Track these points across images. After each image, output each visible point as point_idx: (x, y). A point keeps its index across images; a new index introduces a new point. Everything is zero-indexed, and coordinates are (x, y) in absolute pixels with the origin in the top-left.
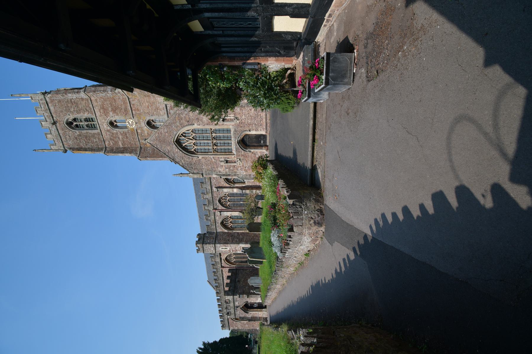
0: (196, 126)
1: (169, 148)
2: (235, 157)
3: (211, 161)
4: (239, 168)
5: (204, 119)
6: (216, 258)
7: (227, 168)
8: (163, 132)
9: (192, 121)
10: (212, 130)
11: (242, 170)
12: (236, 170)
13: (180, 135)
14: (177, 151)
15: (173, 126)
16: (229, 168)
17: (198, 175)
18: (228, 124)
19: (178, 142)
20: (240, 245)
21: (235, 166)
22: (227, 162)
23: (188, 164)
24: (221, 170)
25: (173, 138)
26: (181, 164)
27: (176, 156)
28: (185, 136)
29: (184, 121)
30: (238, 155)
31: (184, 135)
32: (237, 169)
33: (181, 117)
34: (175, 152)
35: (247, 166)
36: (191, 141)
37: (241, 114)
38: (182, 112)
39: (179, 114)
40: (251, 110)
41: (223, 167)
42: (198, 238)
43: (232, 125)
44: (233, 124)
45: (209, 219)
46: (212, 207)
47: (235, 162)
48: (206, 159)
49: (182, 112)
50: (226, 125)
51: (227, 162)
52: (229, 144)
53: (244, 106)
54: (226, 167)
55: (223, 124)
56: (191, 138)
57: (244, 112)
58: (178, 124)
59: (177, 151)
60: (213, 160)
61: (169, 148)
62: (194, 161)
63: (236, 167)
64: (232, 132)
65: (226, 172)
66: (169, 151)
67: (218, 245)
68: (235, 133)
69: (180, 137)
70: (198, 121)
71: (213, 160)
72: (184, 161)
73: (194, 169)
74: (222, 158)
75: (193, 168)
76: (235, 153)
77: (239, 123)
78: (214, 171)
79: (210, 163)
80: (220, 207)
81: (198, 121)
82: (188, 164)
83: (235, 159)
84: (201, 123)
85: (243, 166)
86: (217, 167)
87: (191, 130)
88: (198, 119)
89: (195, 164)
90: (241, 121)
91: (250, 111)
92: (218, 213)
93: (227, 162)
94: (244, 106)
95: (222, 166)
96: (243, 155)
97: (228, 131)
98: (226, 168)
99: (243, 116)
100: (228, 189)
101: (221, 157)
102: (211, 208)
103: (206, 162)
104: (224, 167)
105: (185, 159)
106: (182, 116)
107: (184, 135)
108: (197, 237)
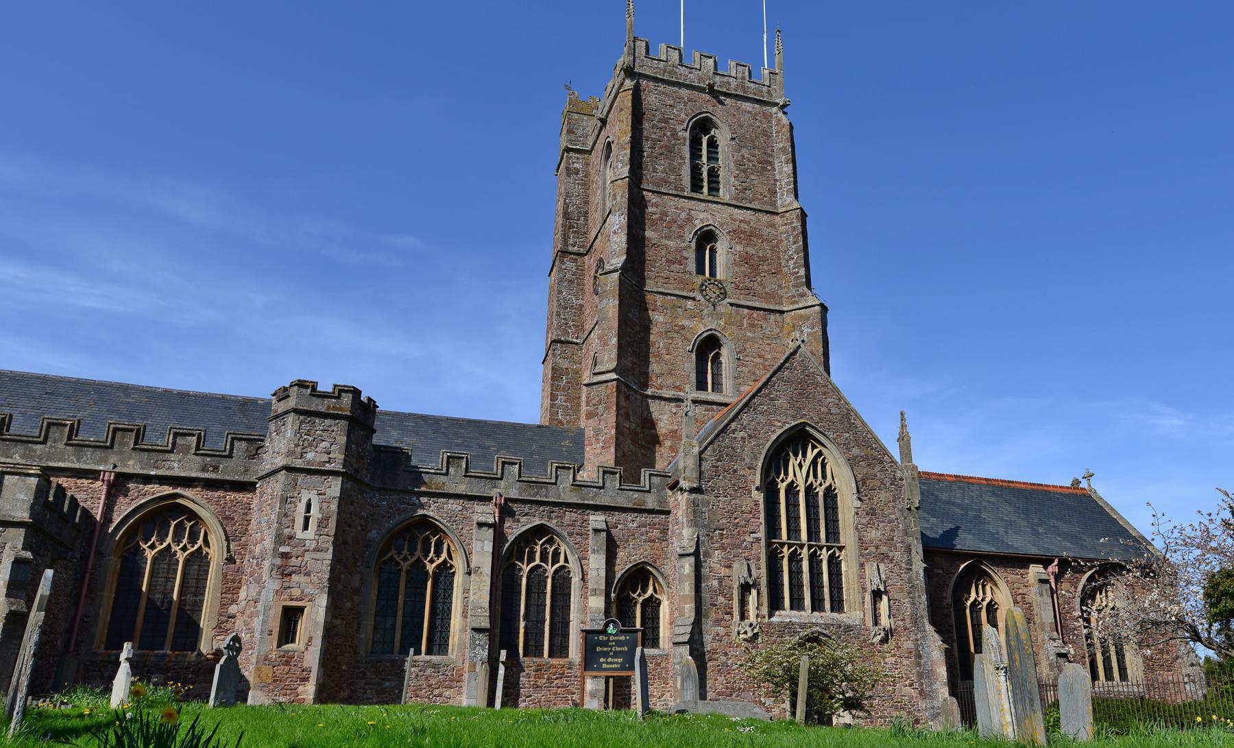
0: (848, 503)
1: (782, 402)
3: (745, 529)
4: (721, 630)
5: (874, 532)
6: (199, 459)
7: (720, 583)
8: (829, 400)
9: (866, 496)
10: (837, 551)
11: (714, 639)
13: (820, 448)
14: (774, 426)
15: (848, 435)
17: (695, 475)
18: (866, 607)
20: (325, 596)
21: (731, 614)
22: (745, 588)
23: (733, 448)
24: (715, 560)
25: (813, 424)
26: (733, 425)
27: (760, 417)
28: (814, 462)
29: (865, 471)
31: (820, 460)
32: (718, 622)
33: (875, 465)
34: (772, 417)
35: (730, 662)
37: (897, 653)
38: (887, 470)
39: (881, 462)
40: (911, 685)
41: (727, 570)
42: (331, 390)
43: (864, 620)
44: (867, 622)
45: (452, 470)
46: (514, 494)
47: (743, 617)
48: (751, 512)
49: (887, 470)
50: (863, 598)
52: (797, 604)
53: (919, 664)
55: (864, 589)
56: (811, 478)
57: (905, 662)
58: (855, 451)
59: (774, 426)
60: (749, 539)
61: (782, 402)
62: (742, 472)
63: (727, 617)
64: (835, 615)
66: (772, 400)
67: (334, 487)
68: (840, 627)
70: (867, 514)
71: (749, 539)
72: (743, 438)
73: (718, 467)
75: (718, 460)
76: (774, 619)
77: (873, 644)
78: (708, 535)
79: (736, 525)
80: (513, 530)
81: (867, 514)
82: (733, 448)
84: (864, 521)
85: (730, 645)
86: (723, 548)
87: (833, 483)
88: (874, 514)
89: (735, 471)
90: (879, 652)
91: (907, 683)
92: (487, 513)
93: (745, 588)
94: (919, 664)
95: (729, 567)
97: (837, 605)
98: (720, 580)
99: (894, 659)
100: (603, 573)
101: (759, 569)
102: (509, 488)
103: (743, 512)
104: (724, 572)
105: (750, 442)
106: (878, 468)
107: (820, 460)
108: (335, 386)
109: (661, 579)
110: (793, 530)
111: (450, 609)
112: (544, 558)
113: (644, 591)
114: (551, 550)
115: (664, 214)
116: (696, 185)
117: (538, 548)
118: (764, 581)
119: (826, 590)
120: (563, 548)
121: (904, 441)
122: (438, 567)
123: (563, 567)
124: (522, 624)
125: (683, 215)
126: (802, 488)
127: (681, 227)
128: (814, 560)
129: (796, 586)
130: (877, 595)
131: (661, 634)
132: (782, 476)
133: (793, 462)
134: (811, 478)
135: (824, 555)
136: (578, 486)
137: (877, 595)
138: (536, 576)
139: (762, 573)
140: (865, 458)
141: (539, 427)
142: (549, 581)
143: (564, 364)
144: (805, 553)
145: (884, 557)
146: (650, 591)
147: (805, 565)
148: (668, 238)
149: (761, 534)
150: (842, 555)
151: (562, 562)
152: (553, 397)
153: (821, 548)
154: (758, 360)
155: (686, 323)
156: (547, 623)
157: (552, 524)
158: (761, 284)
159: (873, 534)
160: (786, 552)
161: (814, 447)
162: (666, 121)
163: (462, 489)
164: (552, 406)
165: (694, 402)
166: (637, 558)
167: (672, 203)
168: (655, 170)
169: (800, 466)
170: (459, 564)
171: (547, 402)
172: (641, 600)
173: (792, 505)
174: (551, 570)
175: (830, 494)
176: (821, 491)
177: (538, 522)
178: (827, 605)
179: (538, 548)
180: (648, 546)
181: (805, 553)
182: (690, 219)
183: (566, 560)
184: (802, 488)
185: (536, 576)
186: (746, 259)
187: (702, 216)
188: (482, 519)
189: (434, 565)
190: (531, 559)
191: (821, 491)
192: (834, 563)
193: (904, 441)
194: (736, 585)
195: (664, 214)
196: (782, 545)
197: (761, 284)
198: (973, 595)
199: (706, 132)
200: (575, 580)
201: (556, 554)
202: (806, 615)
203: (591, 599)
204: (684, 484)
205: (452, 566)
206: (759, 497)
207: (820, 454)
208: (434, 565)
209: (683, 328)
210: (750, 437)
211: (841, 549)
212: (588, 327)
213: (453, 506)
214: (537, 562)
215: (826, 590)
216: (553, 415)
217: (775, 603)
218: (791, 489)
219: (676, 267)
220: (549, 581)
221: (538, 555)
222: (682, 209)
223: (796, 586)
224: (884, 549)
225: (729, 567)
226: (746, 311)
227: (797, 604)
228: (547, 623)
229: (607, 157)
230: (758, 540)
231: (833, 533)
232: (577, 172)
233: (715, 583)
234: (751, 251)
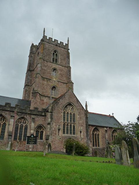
2: (61, 135)
4: (54, 137)
12: (53, 134)
16: (55, 130)
19: (70, 104)
21: (56, 134)
22: (59, 130)
30: (62, 137)
32: (54, 136)
36: (70, 111)
51: (59, 130)
52: (67, 133)
54: (56, 129)
56: (71, 112)
58: (78, 107)
65: (52, 128)
69: (72, 106)
71: (60, 121)
74: (62, 127)
83: (60, 135)
85: (56, 140)
86: (55, 123)
96: (62, 141)
97: (74, 134)
104: (55, 127)
109: (44, 128)
110: (68, 120)
111: (5, 132)
112: (23, 122)
113: (41, 129)
114: (24, 122)
115: (47, 65)
116: (53, 60)
117: (22, 121)
118: (62, 129)
119: (72, 131)
120: (27, 121)
121: (86, 106)
122: (3, 123)
123: (26, 125)
124: (18, 135)
125: (51, 66)
126: (69, 113)
127: (50, 68)
128: (71, 126)
129: (67, 130)
130: (81, 132)
131: (43, 137)
132: (66, 111)
133: (68, 108)
134: (71, 112)
135: (72, 125)
136: (31, 110)
137: (81, 132)
138: (22, 126)
139: (62, 127)
140: (80, 109)
141: (23, 100)
142: (24, 127)
143: (27, 89)
144: (69, 124)
145: (82, 126)
146: (42, 130)
147: (69, 126)
148: (48, 69)
149: (62, 121)
150: (75, 125)
151: (26, 124)
152: (25, 95)
153: (72, 124)
154: (61, 91)
155: (50, 84)
156: (23, 135)
157: (25, 117)
158: (63, 79)
159: (81, 122)
160: (66, 124)
161: (72, 106)
162: (49, 50)
163: (9, 109)
164: (25, 96)
165: (52, 97)
166: (40, 124)
167: (49, 63)
168: (46, 58)
169: (69, 109)
170: (7, 123)
171: (24, 96)
172: (40, 131)
173: (68, 116)
174: (24, 125)
175: (74, 115)
176: (72, 114)
177: (22, 116)
178: (72, 133)
179: (22, 121)
180: (42, 122)
181: (69, 124)
182: (52, 66)
183: (27, 124)
184: (69, 113)
185: (22, 126)
186: (61, 74)
187: (54, 66)
188: (12, 115)
189: (3, 123)
190: (21, 123)
191: (72, 114)
192: (74, 127)
193: (86, 106)
194: (57, 129)
195: (47, 65)
196: (65, 123)
197: (63, 79)
198: (95, 133)
199: (55, 52)
200: (28, 127)
201: (25, 122)
202: (69, 135)
203: (31, 131)
204: (49, 111)
205: (6, 124)
206: (62, 114)
207: (73, 107)
208: (3, 123)
209: (49, 84)
210: (61, 104)
211: (75, 124)
212: (32, 83)
213: (7, 113)
214: (22, 124)
215: (72, 131)
216: (25, 98)
217: (64, 133)
218: (68, 113)
219: (49, 74)
220: (24, 127)
221: (22, 122)
222: (51, 65)
223: (67, 130)
224: (82, 124)
225: (56, 126)
226: (60, 83)
227: (67, 133)
228: (23, 135)
229: (38, 55)
230: (61, 122)
231: (74, 121)
232: (32, 57)
233: (54, 129)
234: (61, 73)
